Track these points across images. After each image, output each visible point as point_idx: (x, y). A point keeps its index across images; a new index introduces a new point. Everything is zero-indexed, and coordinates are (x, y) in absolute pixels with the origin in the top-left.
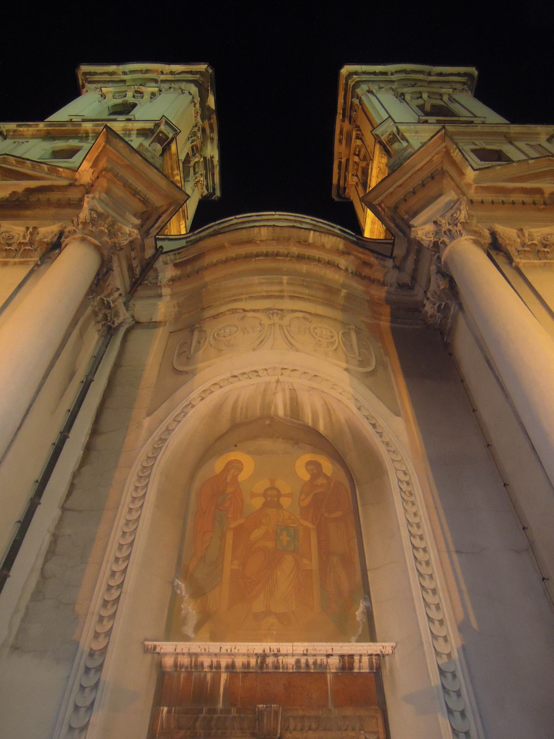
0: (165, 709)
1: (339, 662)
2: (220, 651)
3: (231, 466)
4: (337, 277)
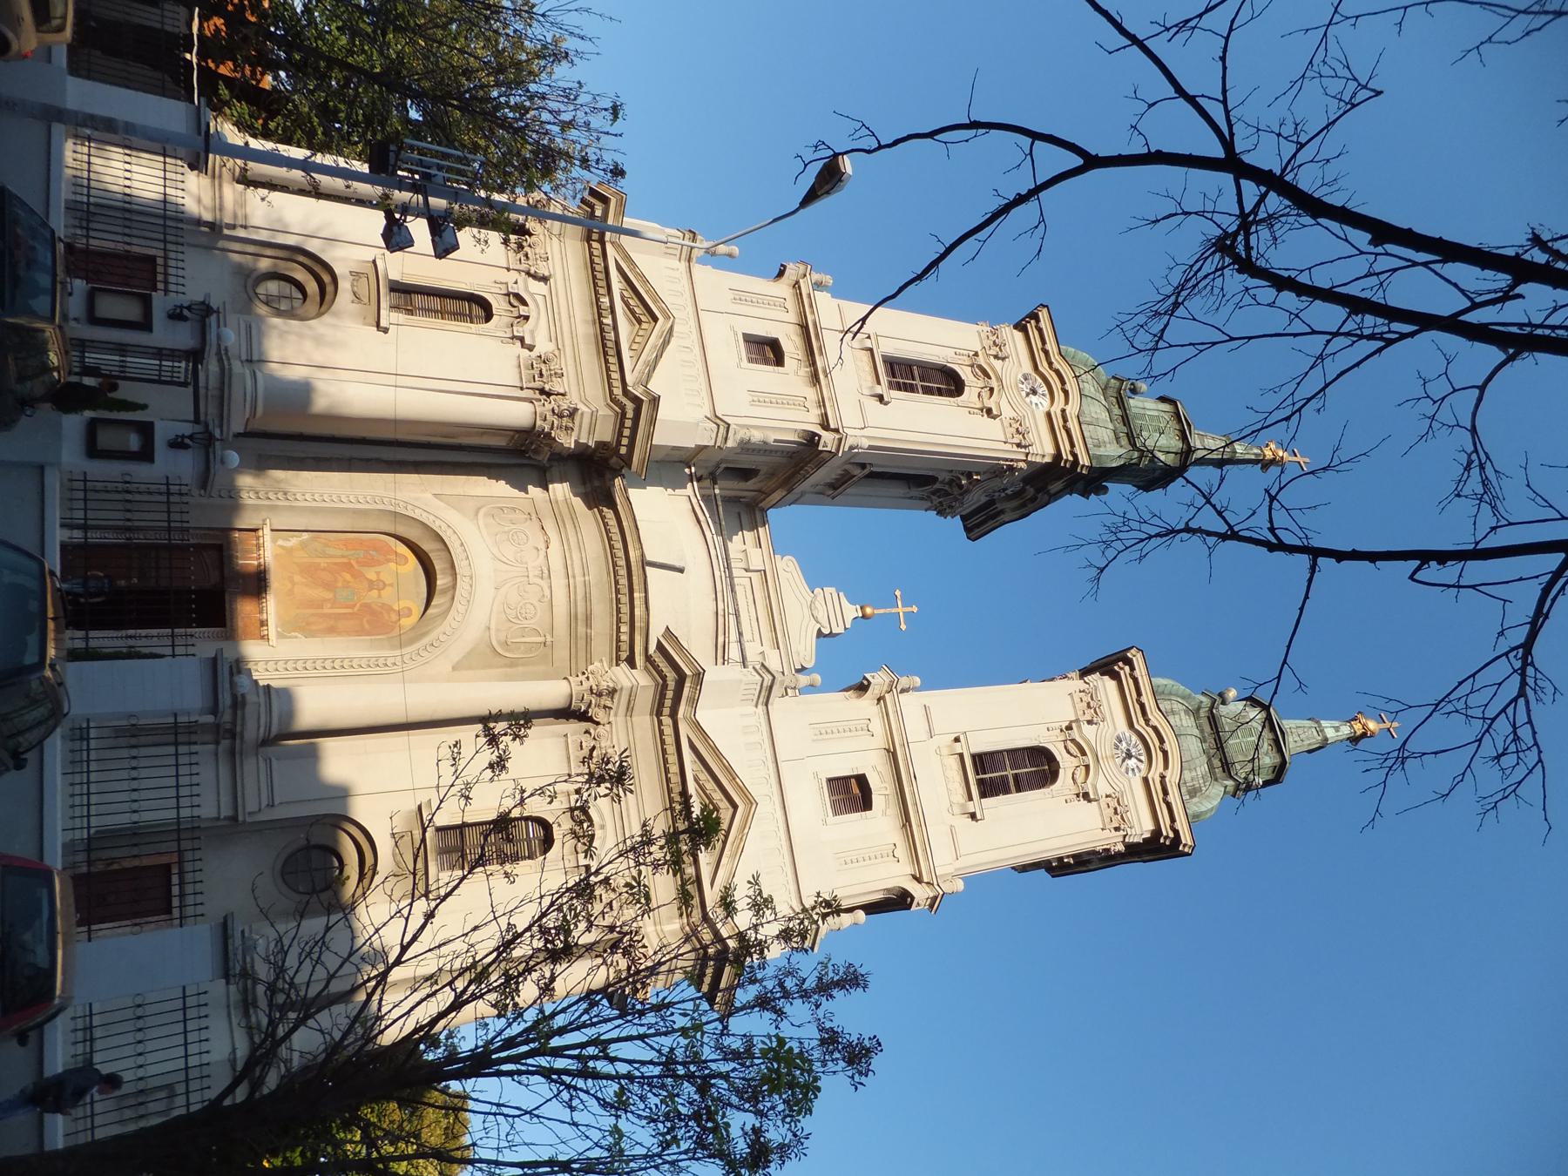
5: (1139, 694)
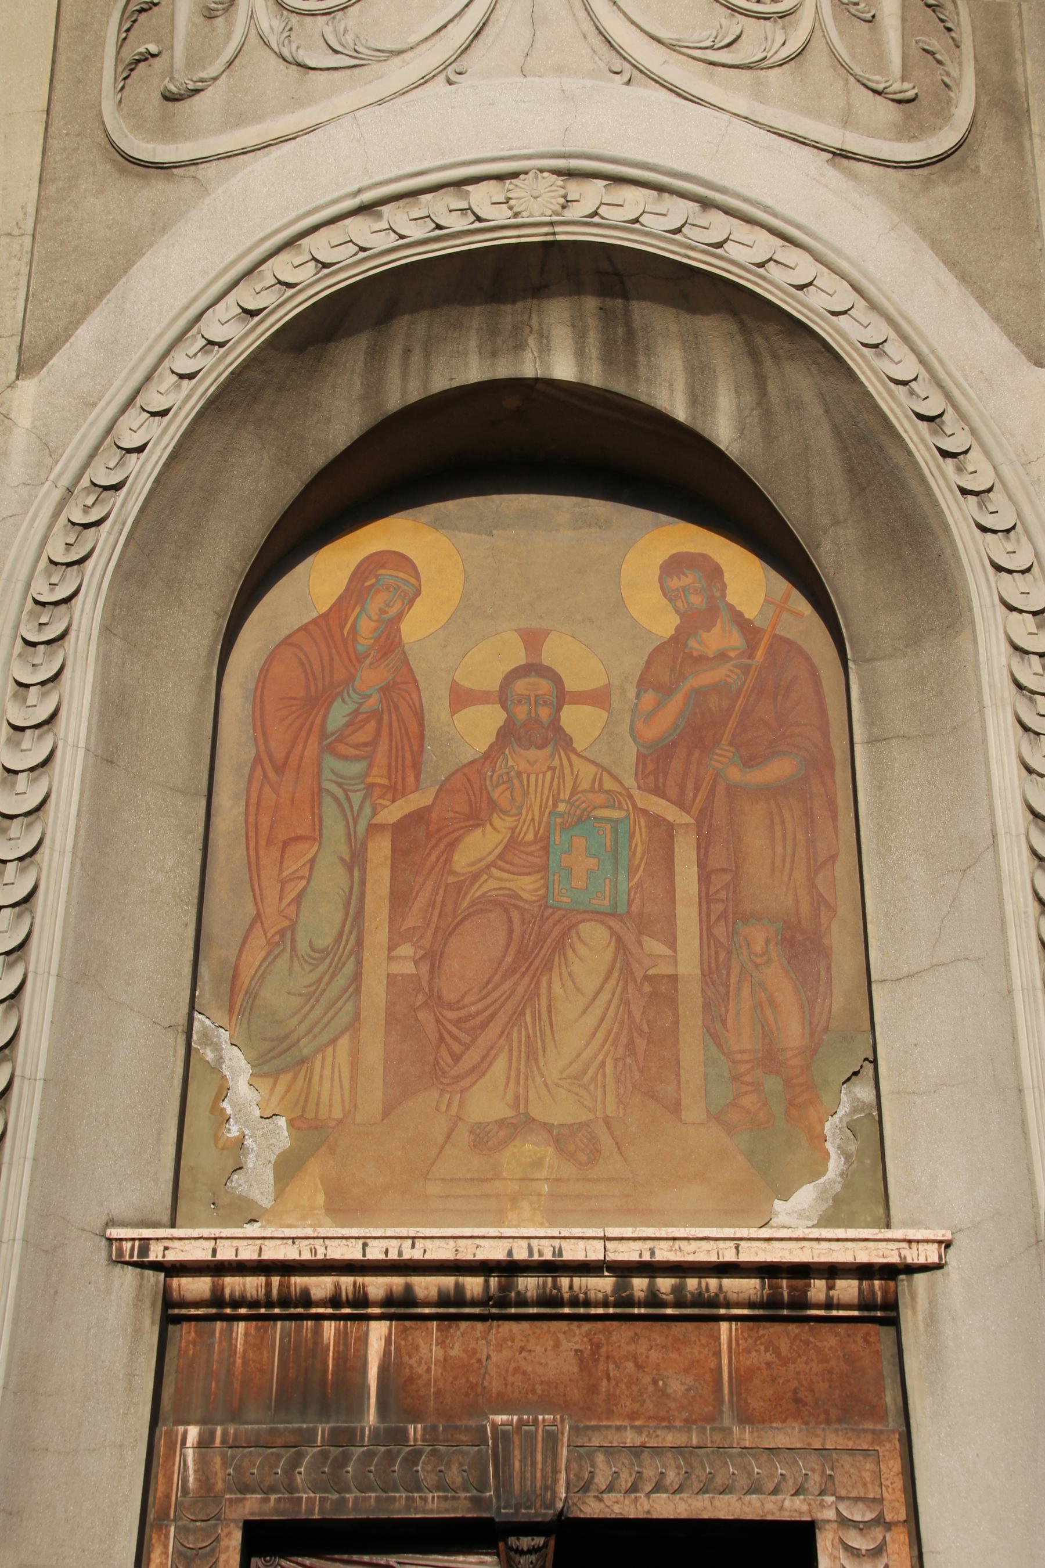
0: (193, 1432)
1: (758, 1287)
2: (364, 1255)
3: (374, 580)
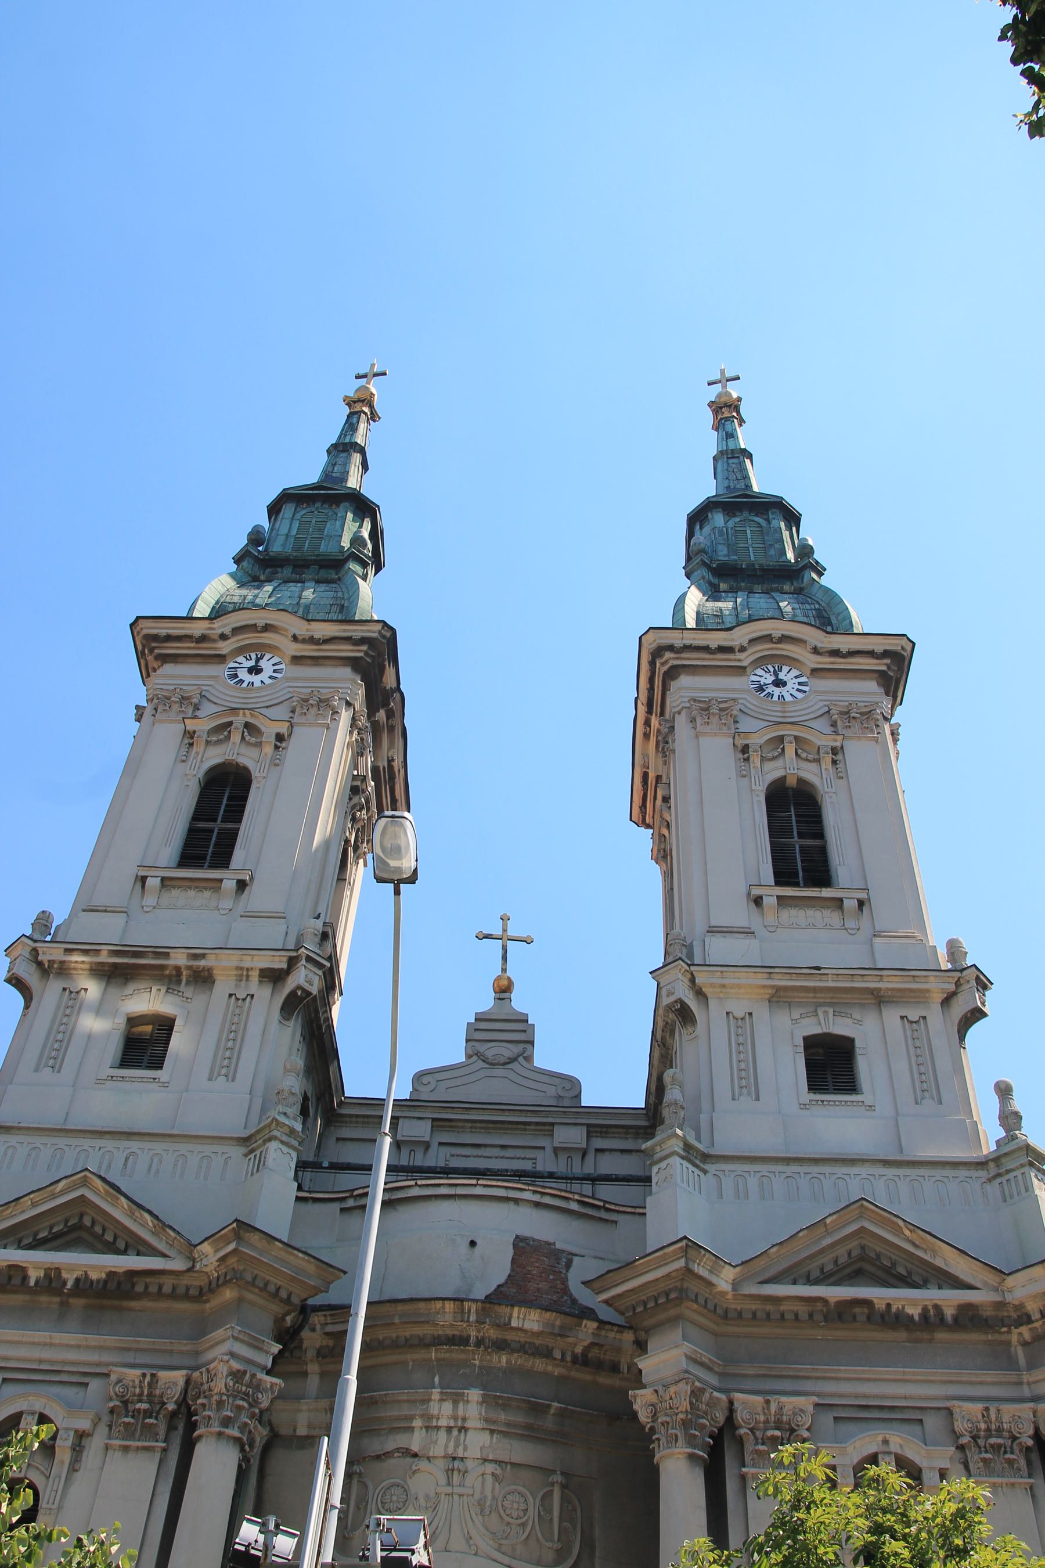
4: (550, 1368)
5: (706, 649)
